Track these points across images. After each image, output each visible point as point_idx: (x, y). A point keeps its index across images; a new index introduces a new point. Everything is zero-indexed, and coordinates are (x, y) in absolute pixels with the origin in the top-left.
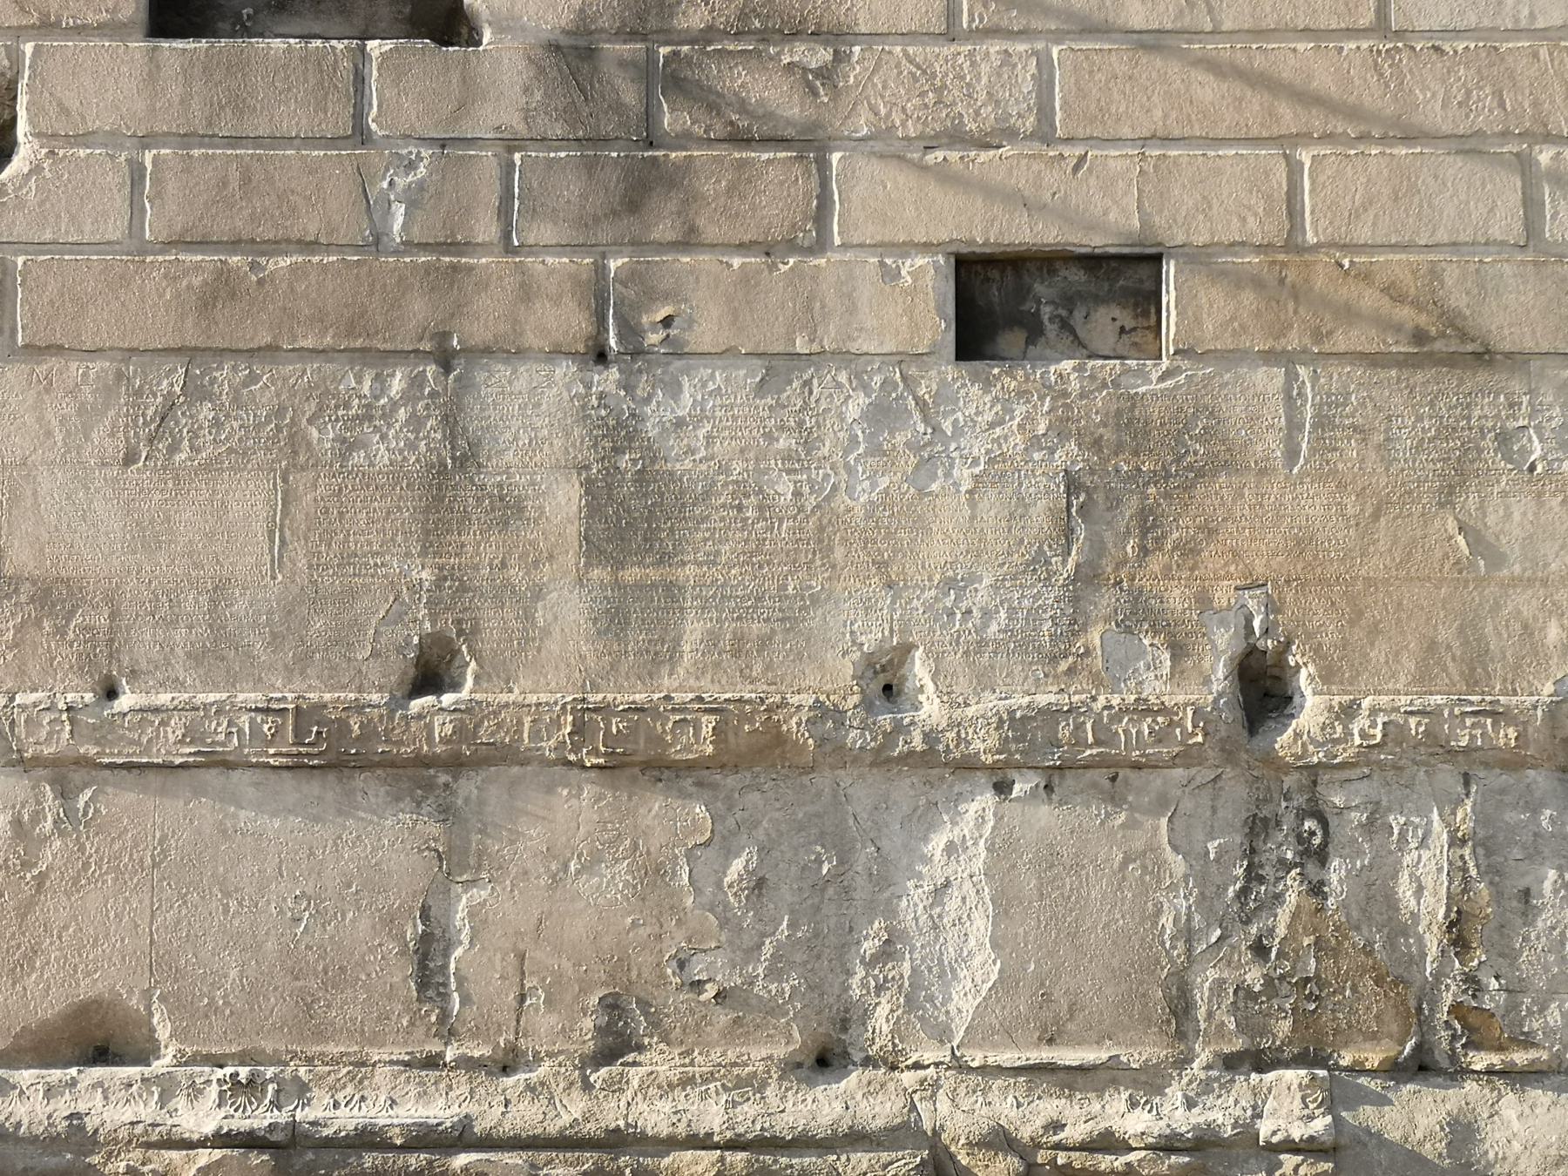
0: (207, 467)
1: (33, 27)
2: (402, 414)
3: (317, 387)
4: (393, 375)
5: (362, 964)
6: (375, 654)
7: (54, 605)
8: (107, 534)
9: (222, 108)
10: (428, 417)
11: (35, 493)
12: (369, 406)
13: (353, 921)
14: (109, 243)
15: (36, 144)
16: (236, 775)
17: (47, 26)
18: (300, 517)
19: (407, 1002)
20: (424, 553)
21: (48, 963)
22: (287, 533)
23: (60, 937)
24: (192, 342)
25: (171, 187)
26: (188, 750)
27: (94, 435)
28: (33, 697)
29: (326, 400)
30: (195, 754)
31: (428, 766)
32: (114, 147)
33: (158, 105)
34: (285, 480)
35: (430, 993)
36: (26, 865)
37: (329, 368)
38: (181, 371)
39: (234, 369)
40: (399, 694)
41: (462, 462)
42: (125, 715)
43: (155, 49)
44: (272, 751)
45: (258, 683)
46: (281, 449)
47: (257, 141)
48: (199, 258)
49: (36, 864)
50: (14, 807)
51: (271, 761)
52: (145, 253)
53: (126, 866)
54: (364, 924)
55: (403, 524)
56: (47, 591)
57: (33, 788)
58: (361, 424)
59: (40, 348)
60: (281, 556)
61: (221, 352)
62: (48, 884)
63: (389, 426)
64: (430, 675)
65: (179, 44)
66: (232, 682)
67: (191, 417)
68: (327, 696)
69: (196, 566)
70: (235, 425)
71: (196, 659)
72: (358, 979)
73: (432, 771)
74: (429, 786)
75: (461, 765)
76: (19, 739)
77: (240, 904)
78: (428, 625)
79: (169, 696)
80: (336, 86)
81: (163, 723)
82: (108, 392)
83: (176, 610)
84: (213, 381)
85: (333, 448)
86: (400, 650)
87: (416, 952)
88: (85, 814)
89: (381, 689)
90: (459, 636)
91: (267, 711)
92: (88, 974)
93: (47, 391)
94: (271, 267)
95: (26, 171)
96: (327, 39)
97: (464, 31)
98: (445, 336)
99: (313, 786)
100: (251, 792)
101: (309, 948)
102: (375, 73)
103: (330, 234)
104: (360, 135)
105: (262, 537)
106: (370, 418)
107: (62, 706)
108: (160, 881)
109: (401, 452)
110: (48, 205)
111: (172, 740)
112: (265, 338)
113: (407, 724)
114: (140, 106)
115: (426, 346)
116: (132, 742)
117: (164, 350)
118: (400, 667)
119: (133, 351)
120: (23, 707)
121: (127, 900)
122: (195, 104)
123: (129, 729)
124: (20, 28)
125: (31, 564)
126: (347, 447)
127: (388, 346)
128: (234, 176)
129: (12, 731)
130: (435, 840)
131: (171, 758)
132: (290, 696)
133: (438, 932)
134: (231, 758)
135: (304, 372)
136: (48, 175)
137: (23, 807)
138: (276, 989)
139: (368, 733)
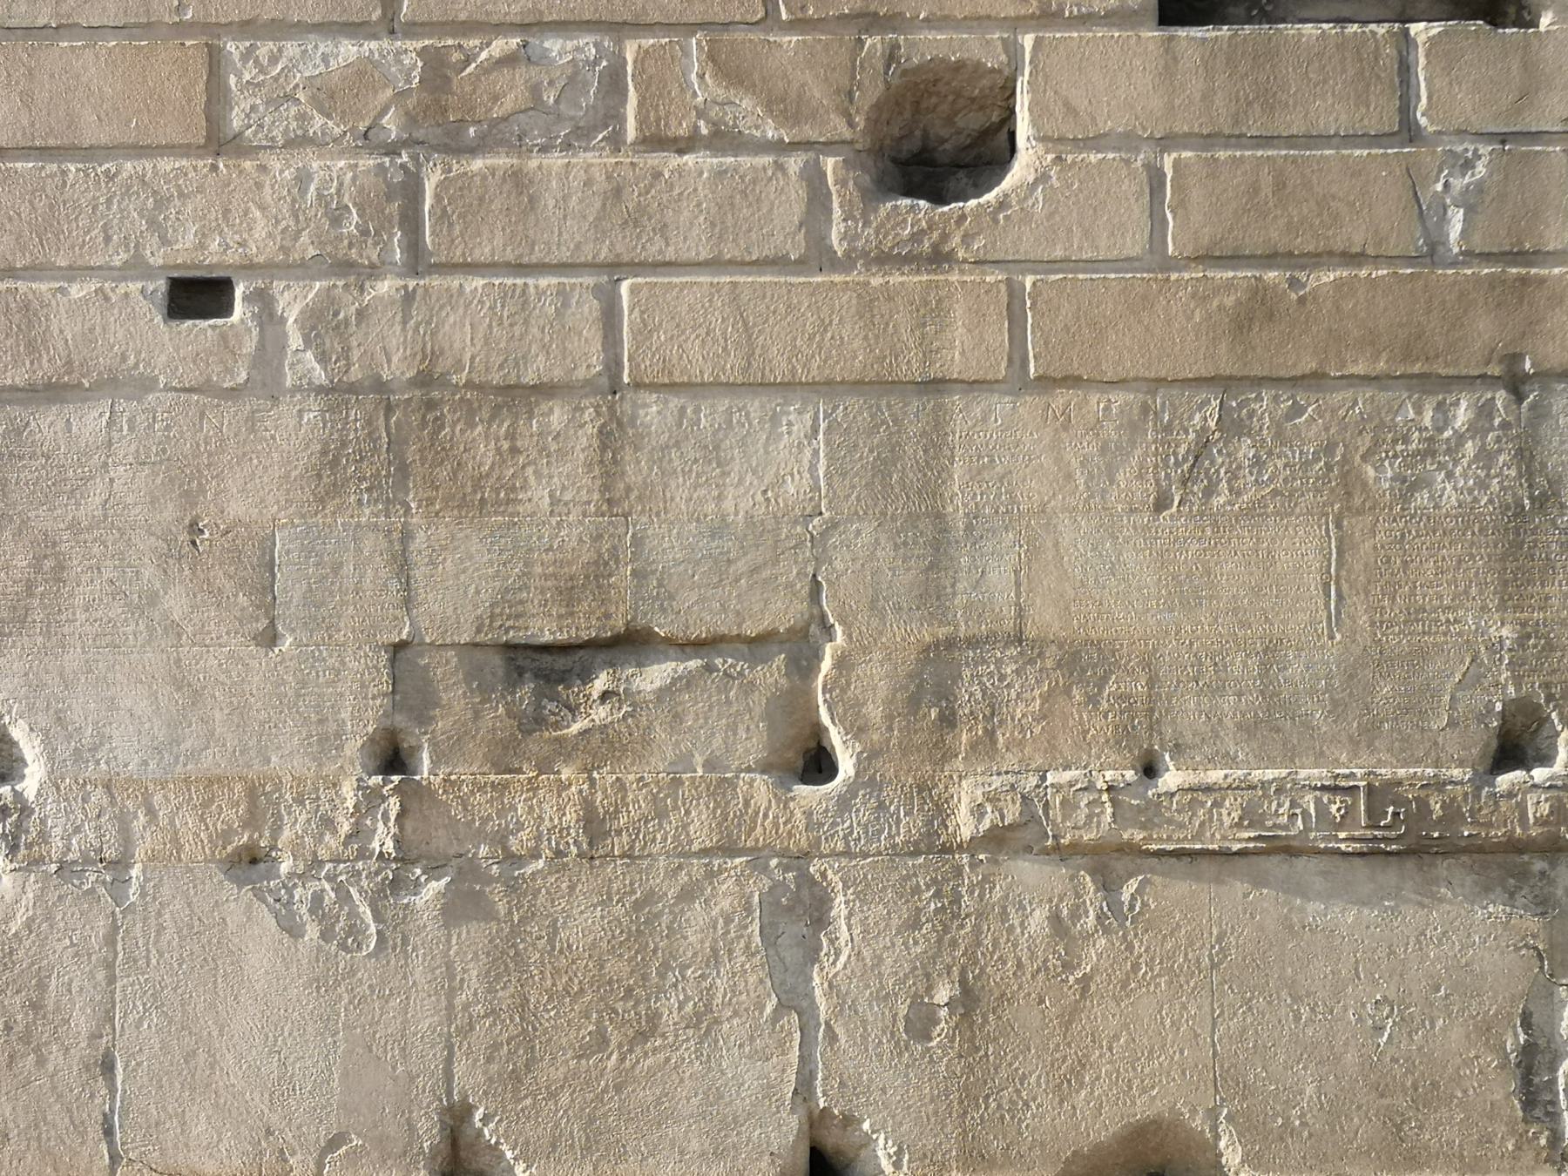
0: (1253, 512)
1: (1032, 16)
2: (1470, 448)
3: (1371, 418)
4: (1457, 404)
5: (1457, 1079)
6: (1452, 723)
7: (1084, 671)
8: (1140, 589)
9: (1249, 104)
10: (1500, 451)
11: (1056, 544)
12: (1431, 439)
13: (1444, 1029)
14: (1127, 259)
15: (1040, 149)
16: (1301, 863)
17: (1047, 17)
18: (1358, 567)
19: (1511, 1123)
20: (1502, 607)
21: (1098, 1078)
22: (1345, 587)
23: (1110, 1049)
24: (1227, 369)
25: (1196, 195)
26: (1246, 835)
27: (1120, 477)
28: (1067, 776)
29: (1384, 436)
30: (1250, 839)
31: (1521, 852)
32: (1128, 150)
33: (1177, 102)
34: (1339, 526)
35: (1538, 1112)
36: (1068, 967)
37: (1383, 397)
38: (1215, 403)
39: (1276, 399)
40: (1481, 769)
41: (1541, 503)
42: (1173, 795)
43: (1171, 38)
44: (1342, 835)
45: (1320, 758)
46: (1332, 490)
47: (1290, 141)
48: (1231, 274)
49: (1079, 965)
50: (1051, 901)
51: (1343, 846)
52: (1169, 269)
53: (1181, 967)
54: (1456, 1034)
55: (1477, 573)
56: (1076, 655)
57: (1072, 879)
58: (1423, 461)
59: (1055, 380)
60: (1338, 613)
61: (1259, 382)
62: (1093, 988)
63: (1456, 462)
64: (1515, 746)
65: (1197, 32)
66: (1290, 757)
67: (1229, 455)
68: (1402, 772)
69: (1245, 624)
70: (1280, 463)
71: (1248, 731)
72: (1453, 1096)
73: (1526, 858)
74: (1523, 874)
75: (1560, 850)
76: (1054, 824)
77: (1313, 1010)
78: (1511, 689)
79: (1222, 773)
80: (1378, 77)
81: (1215, 804)
82: (1134, 429)
83: (1223, 675)
84: (1251, 414)
85: (1392, 488)
86: (1481, 718)
87: (1518, 1065)
88: (1132, 908)
89: (1461, 764)
90: (1548, 701)
91: (1334, 789)
92: (1144, 1091)
93: (1065, 428)
94: (1312, 283)
95: (1031, 179)
96: (1365, 22)
97: (1512, 10)
98: (1517, 358)
99: (1390, 875)
100: (1318, 883)
101: (1394, 1060)
102: (1422, 61)
103: (1379, 244)
104: (1409, 132)
105: (1315, 591)
106: (1433, 454)
107: (1100, 784)
108: (1221, 984)
109: (1470, 491)
110: (1058, 218)
111: (1227, 821)
112: (1309, 365)
113: (1496, 803)
114: (1157, 103)
115: (1495, 370)
116: (1181, 826)
117: (1195, 380)
118: (1482, 738)
119: (1160, 381)
120: (1058, 788)
121: (1184, 1007)
122: (1219, 101)
123: (1179, 811)
124: (1018, 18)
125: (1056, 625)
126: (1408, 487)
127: (1451, 371)
128: (1266, 182)
129: (1046, 814)
130: (1534, 936)
131: (1227, 844)
132: (1359, 772)
133: (1542, 1042)
134: (1295, 843)
135: (1355, 403)
136: (1056, 184)
137: (1061, 900)
138: (1359, 1107)
139: (1452, 815)
